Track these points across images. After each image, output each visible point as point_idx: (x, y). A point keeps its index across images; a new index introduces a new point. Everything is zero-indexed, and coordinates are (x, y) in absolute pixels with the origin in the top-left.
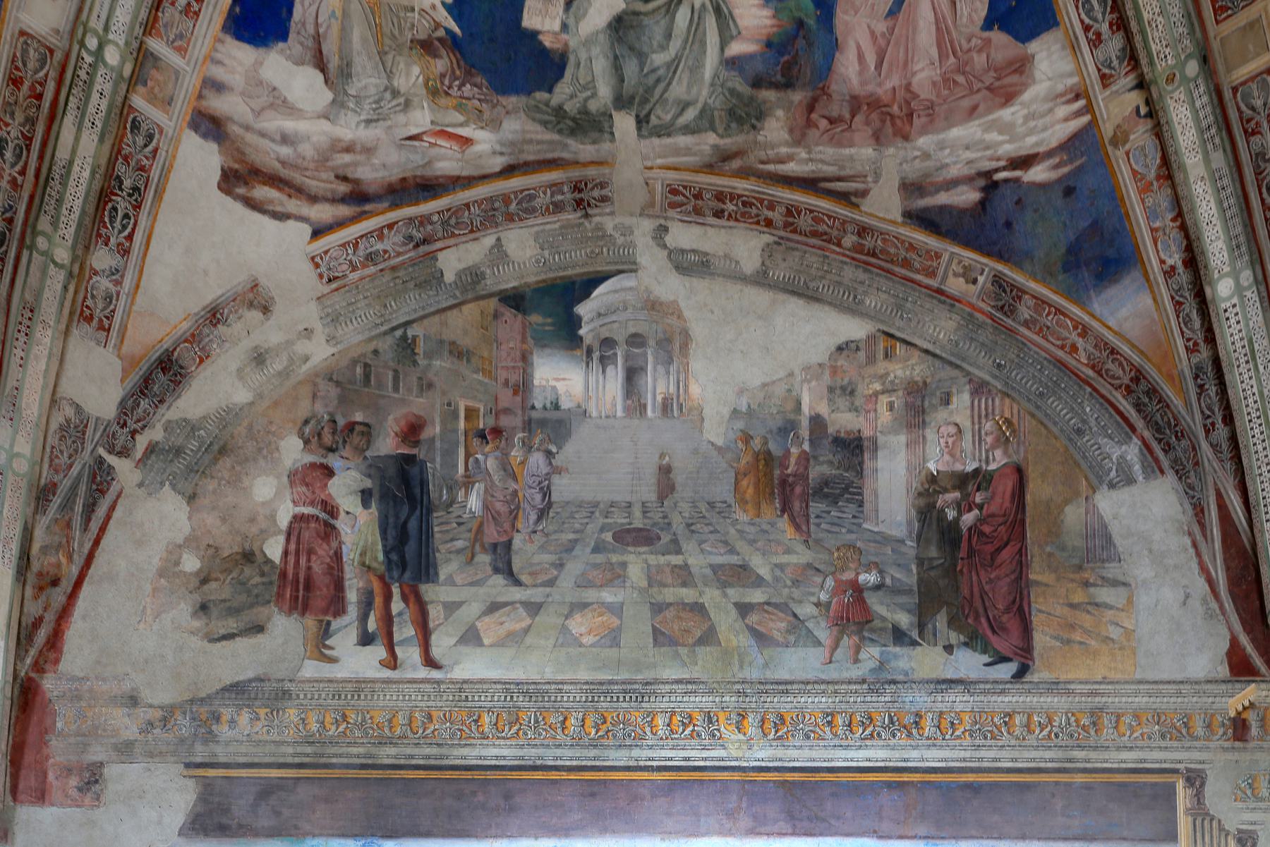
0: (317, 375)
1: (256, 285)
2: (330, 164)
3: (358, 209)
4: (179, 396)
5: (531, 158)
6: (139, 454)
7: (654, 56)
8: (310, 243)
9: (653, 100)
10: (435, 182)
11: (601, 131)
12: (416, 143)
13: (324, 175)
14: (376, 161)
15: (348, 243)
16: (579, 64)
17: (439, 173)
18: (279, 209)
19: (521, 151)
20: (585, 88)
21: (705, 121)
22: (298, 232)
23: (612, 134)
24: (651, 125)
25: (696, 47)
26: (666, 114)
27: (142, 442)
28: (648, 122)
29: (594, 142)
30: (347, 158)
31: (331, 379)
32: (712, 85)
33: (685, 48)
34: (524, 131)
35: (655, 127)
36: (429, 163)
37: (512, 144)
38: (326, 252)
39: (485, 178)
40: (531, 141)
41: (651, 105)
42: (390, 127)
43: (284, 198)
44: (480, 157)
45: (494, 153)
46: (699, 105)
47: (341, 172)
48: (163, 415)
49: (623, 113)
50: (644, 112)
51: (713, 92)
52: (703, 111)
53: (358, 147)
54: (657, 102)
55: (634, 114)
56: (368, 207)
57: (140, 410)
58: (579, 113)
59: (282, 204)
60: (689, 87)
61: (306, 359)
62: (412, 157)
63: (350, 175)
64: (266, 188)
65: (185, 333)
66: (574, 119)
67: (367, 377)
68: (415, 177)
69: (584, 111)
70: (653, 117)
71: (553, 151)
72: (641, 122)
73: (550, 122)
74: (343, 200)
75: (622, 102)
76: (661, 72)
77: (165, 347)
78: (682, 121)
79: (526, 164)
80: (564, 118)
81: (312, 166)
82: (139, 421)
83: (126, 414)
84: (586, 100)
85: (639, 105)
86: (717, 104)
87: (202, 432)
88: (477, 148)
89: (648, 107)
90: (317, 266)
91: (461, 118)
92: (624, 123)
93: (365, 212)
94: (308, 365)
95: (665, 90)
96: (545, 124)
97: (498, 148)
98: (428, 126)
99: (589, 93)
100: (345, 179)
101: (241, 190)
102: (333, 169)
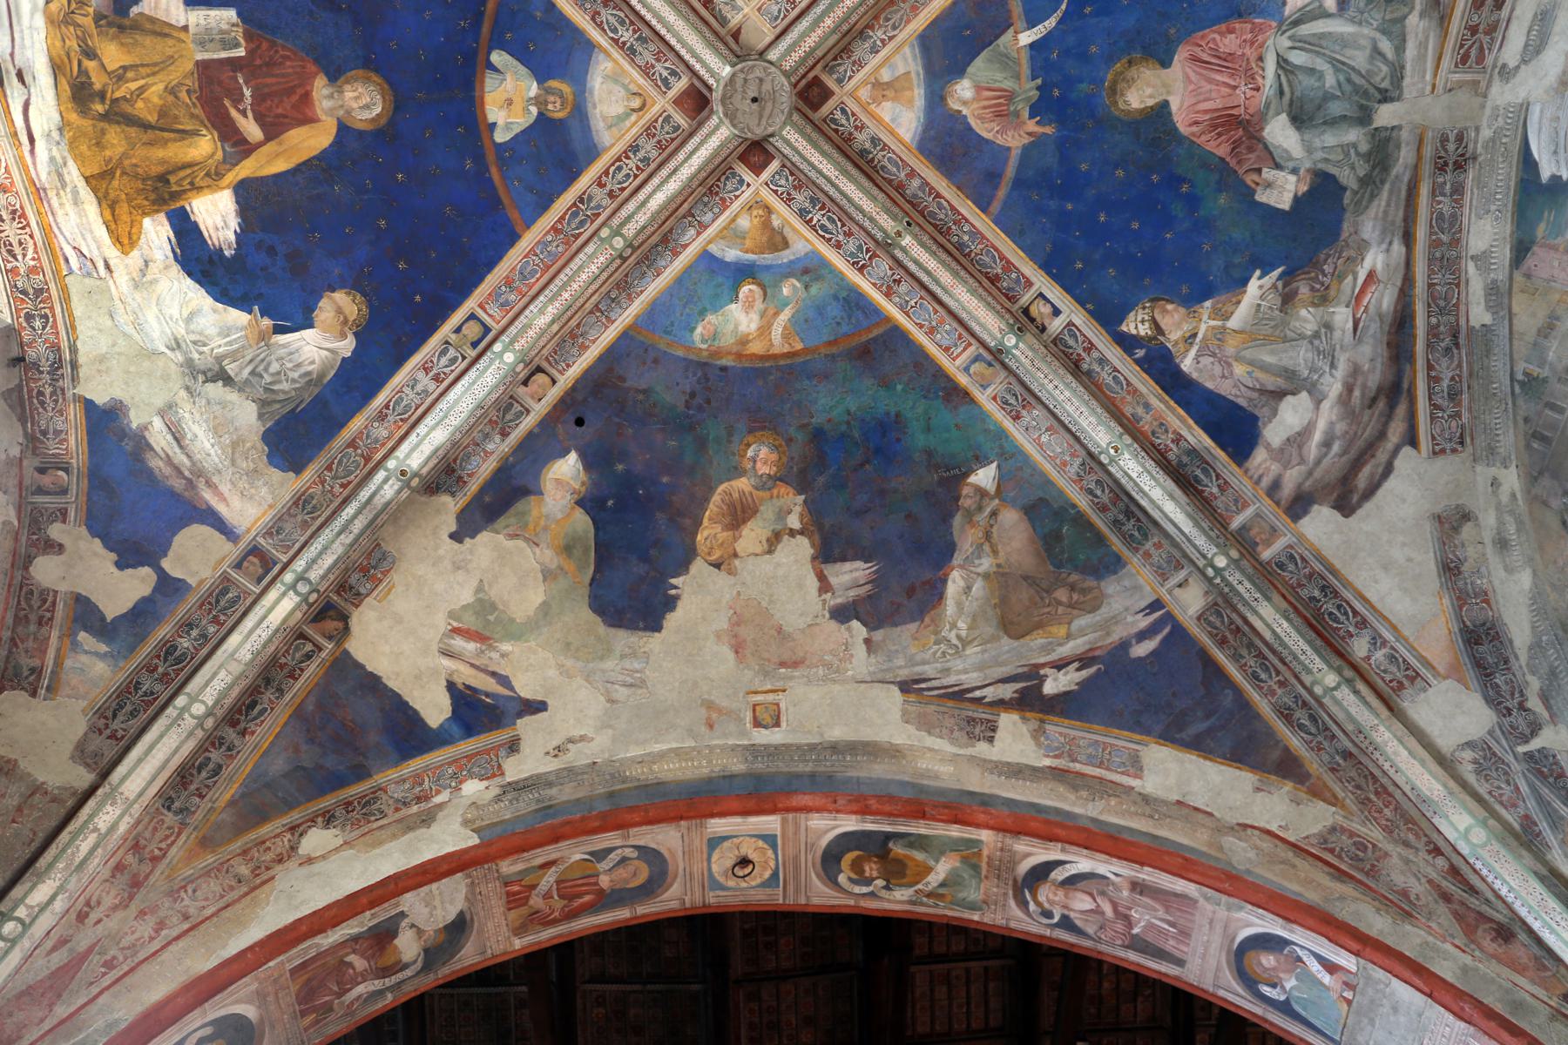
0: (1529, 492)
1: (1439, 517)
2: (1357, 410)
3: (1405, 395)
4: (1511, 642)
5: (1401, 214)
6: (1546, 714)
7: (1327, 85)
8: (1419, 452)
9: (1366, 86)
10: (1399, 315)
11: (1388, 140)
12: (1361, 325)
13: (1366, 418)
14: (1366, 367)
15: (1431, 414)
16: (1326, 160)
17: (1392, 308)
18: (1380, 470)
19: (1393, 223)
20: (1347, 155)
21: (1395, 30)
22: (1406, 461)
23: (1393, 128)
24: (1390, 88)
25: (1324, 43)
26: (1381, 71)
27: (1534, 703)
28: (1386, 91)
29: (1398, 147)
30: (1357, 393)
31: (1536, 479)
32: (1360, 24)
33: (1324, 54)
34: (1376, 218)
35: (1392, 83)
36: (1380, 316)
37: (1384, 232)
38: (1433, 438)
39: (1409, 263)
40: (1386, 213)
41: (1370, 87)
42: (1342, 347)
43: (1373, 462)
44: (1388, 265)
45: (1388, 250)
46: (1378, 35)
47: (1367, 402)
48: (1521, 667)
49: (1375, 117)
50: (1378, 96)
51: (1367, 22)
52: (1384, 32)
53: (1351, 380)
54: (1368, 81)
55: (1377, 106)
56: (1405, 386)
57: (1504, 687)
58: (1368, 161)
59: (1378, 466)
60: (1360, 48)
61: (1513, 495)
62: (1371, 331)
63: (1372, 395)
64: (1360, 475)
65: (1453, 605)
66: (1374, 168)
67: (1544, 439)
68: (1389, 332)
69: (1367, 157)
70: (1384, 85)
71: (1400, 190)
72: (1385, 97)
73: (1372, 191)
74: (1392, 406)
75: (1363, 117)
76: (1342, 78)
77: (1456, 630)
78: (1390, 54)
79: (1406, 220)
80: (1371, 177)
81: (1354, 427)
82: (1513, 694)
83: (1500, 703)
84: (1358, 154)
85: (1369, 99)
86: (1378, 16)
87: (1544, 638)
88: (1379, 267)
89: (1372, 90)
90: (1443, 451)
91: (1350, 278)
92: (1385, 115)
93: (1409, 390)
94: (1519, 496)
95: (1359, 73)
96: (1373, 197)
97: (1384, 246)
98: (1349, 310)
99: (1352, 151)
100: (1374, 400)
101: (1355, 498)
102: (1363, 409)
